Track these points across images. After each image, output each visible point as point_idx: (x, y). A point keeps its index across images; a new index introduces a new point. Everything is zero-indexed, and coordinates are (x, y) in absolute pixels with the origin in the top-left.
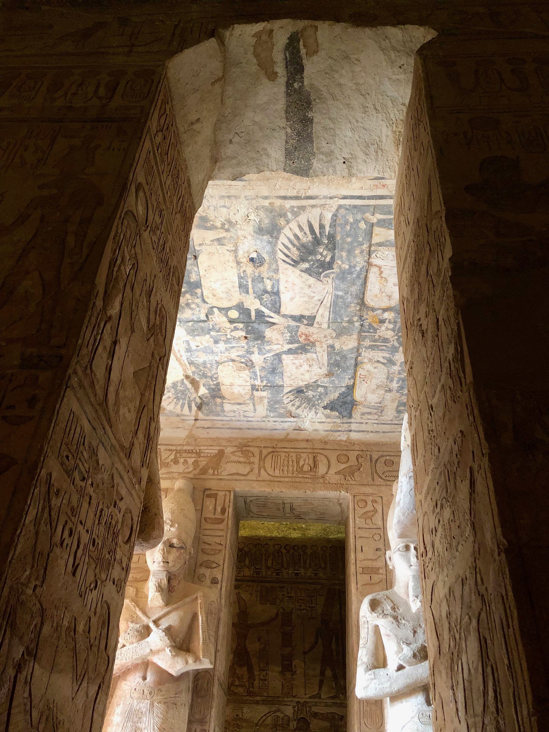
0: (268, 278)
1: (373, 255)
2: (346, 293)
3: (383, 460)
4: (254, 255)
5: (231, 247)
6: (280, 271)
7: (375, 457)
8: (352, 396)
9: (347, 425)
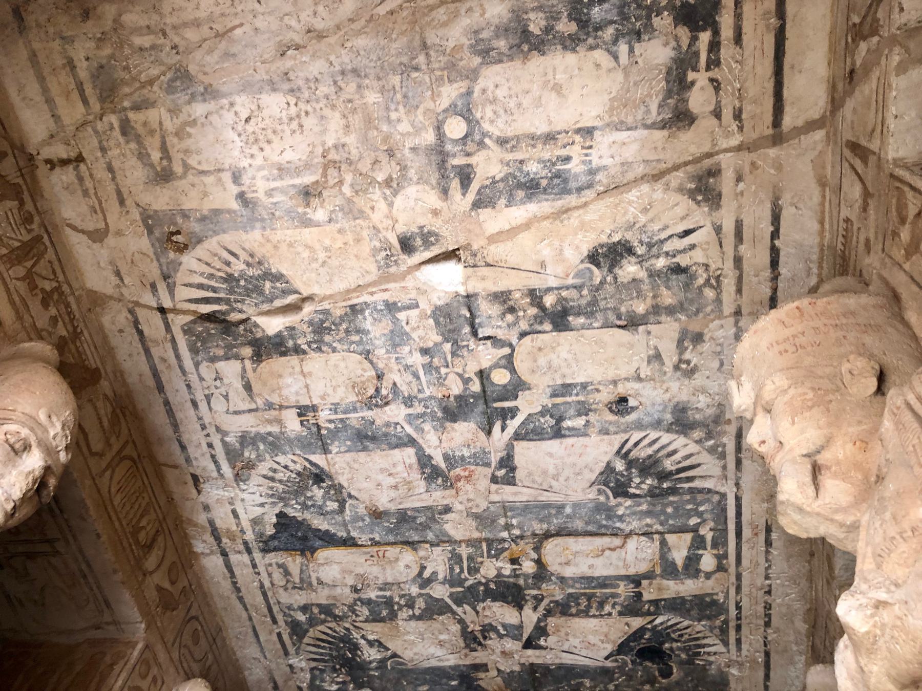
0: (588, 421)
1: (643, 538)
2: (568, 516)
3: (196, 624)
4: (632, 402)
5: (645, 371)
6: (606, 437)
7: (193, 612)
8: (322, 547)
9: (242, 547)
